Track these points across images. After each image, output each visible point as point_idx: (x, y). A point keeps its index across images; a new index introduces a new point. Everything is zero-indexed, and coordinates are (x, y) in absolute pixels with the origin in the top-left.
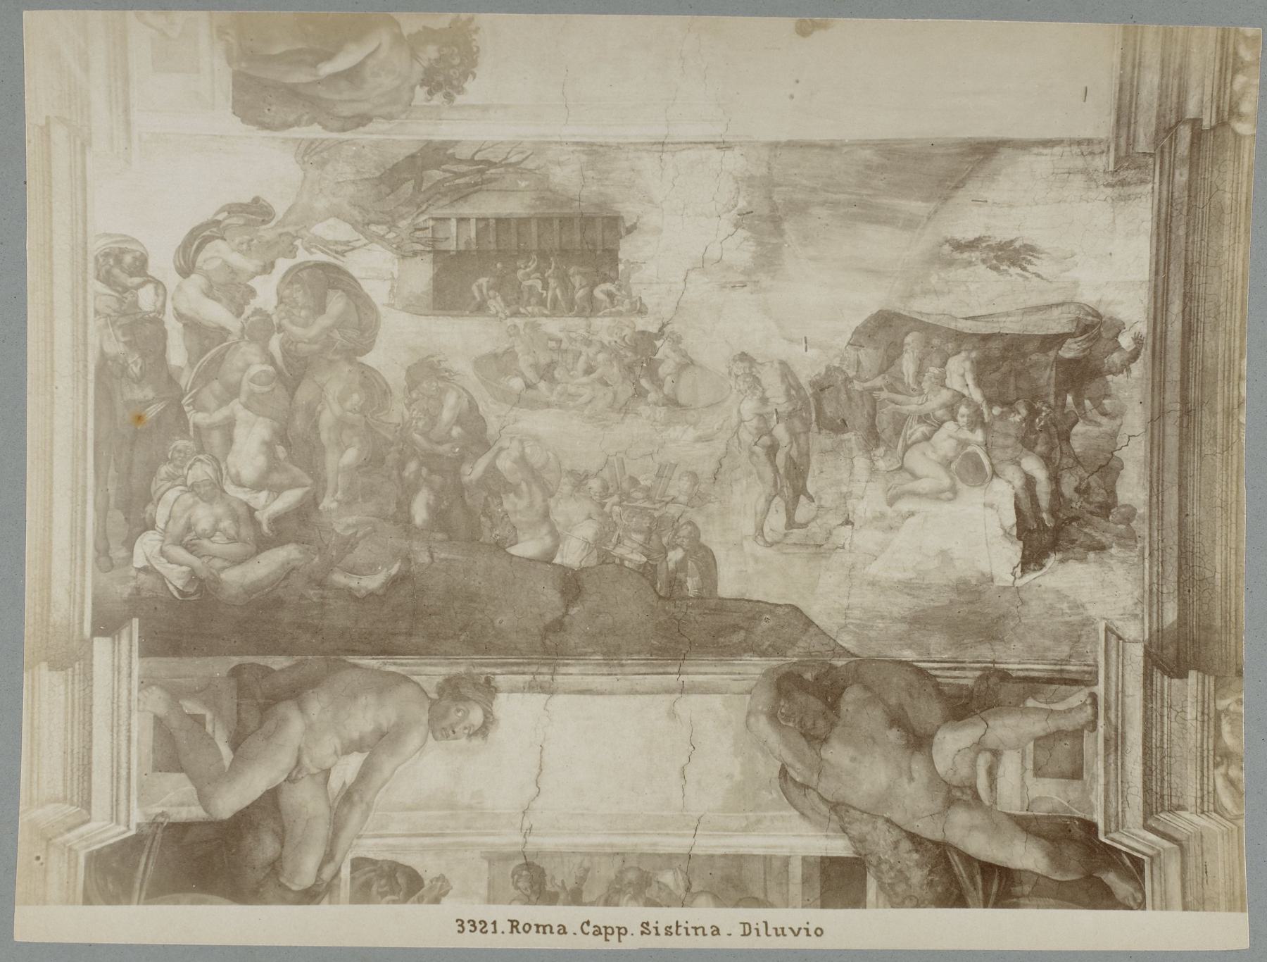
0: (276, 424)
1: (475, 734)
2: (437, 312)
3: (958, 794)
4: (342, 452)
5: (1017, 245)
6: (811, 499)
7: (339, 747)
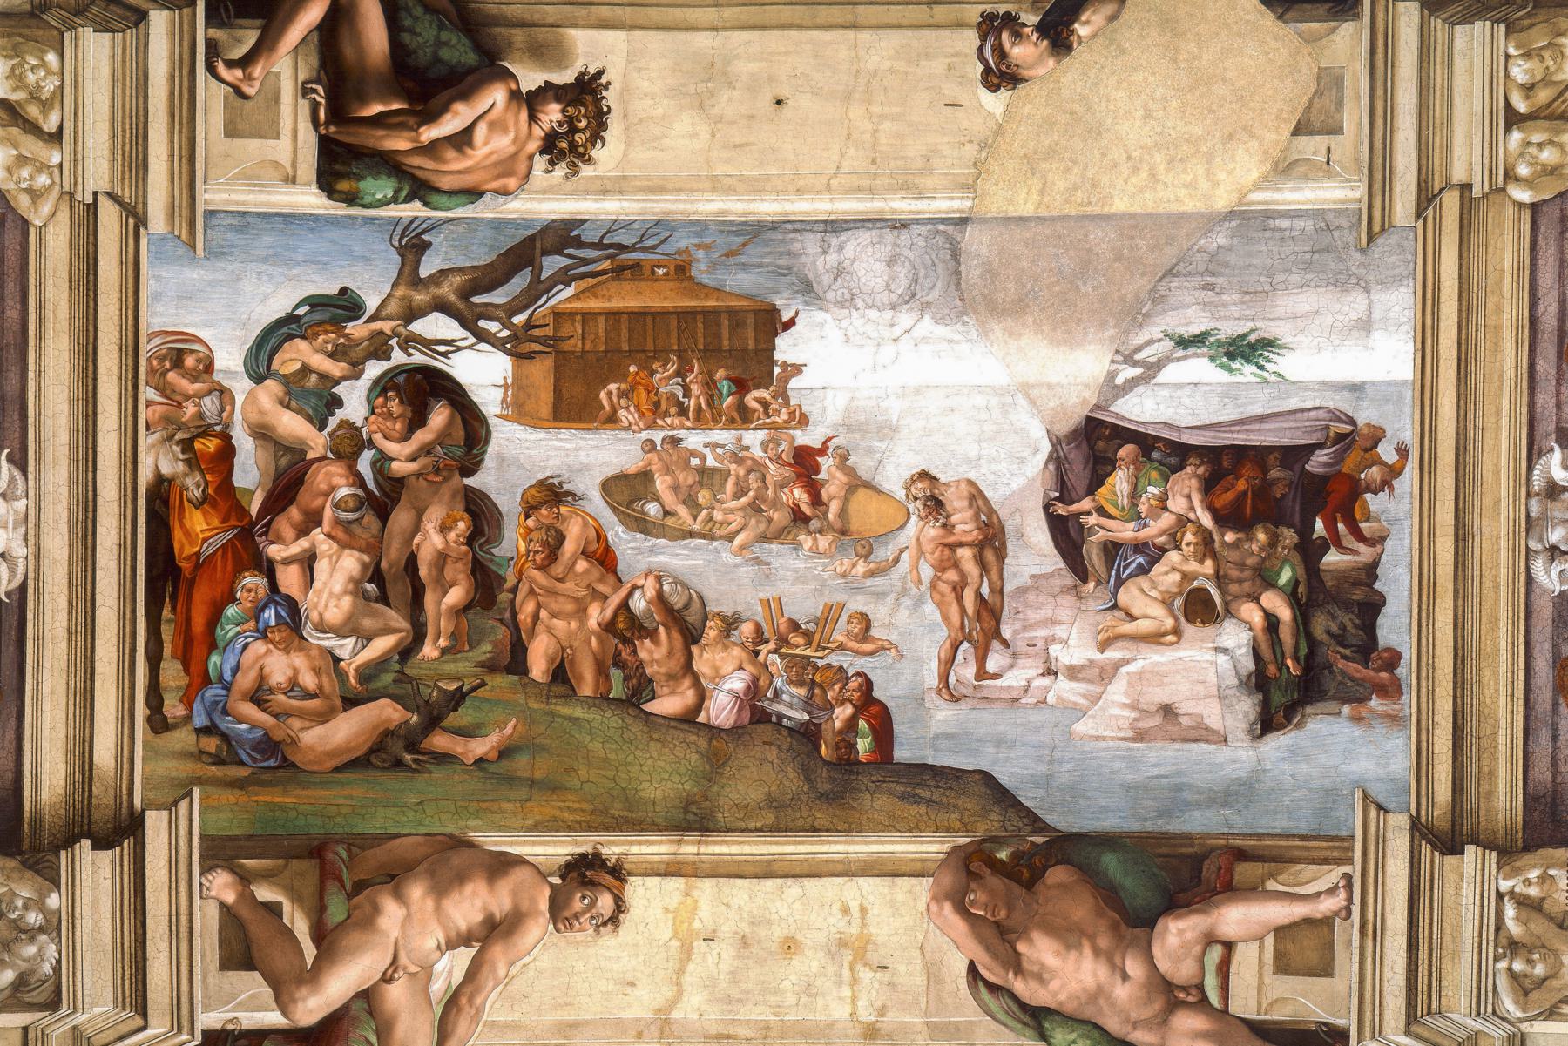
0: (366, 558)
1: (605, 924)
2: (557, 425)
3: (1182, 996)
4: (445, 593)
5: (1252, 338)
6: (1005, 643)
7: (443, 942)
